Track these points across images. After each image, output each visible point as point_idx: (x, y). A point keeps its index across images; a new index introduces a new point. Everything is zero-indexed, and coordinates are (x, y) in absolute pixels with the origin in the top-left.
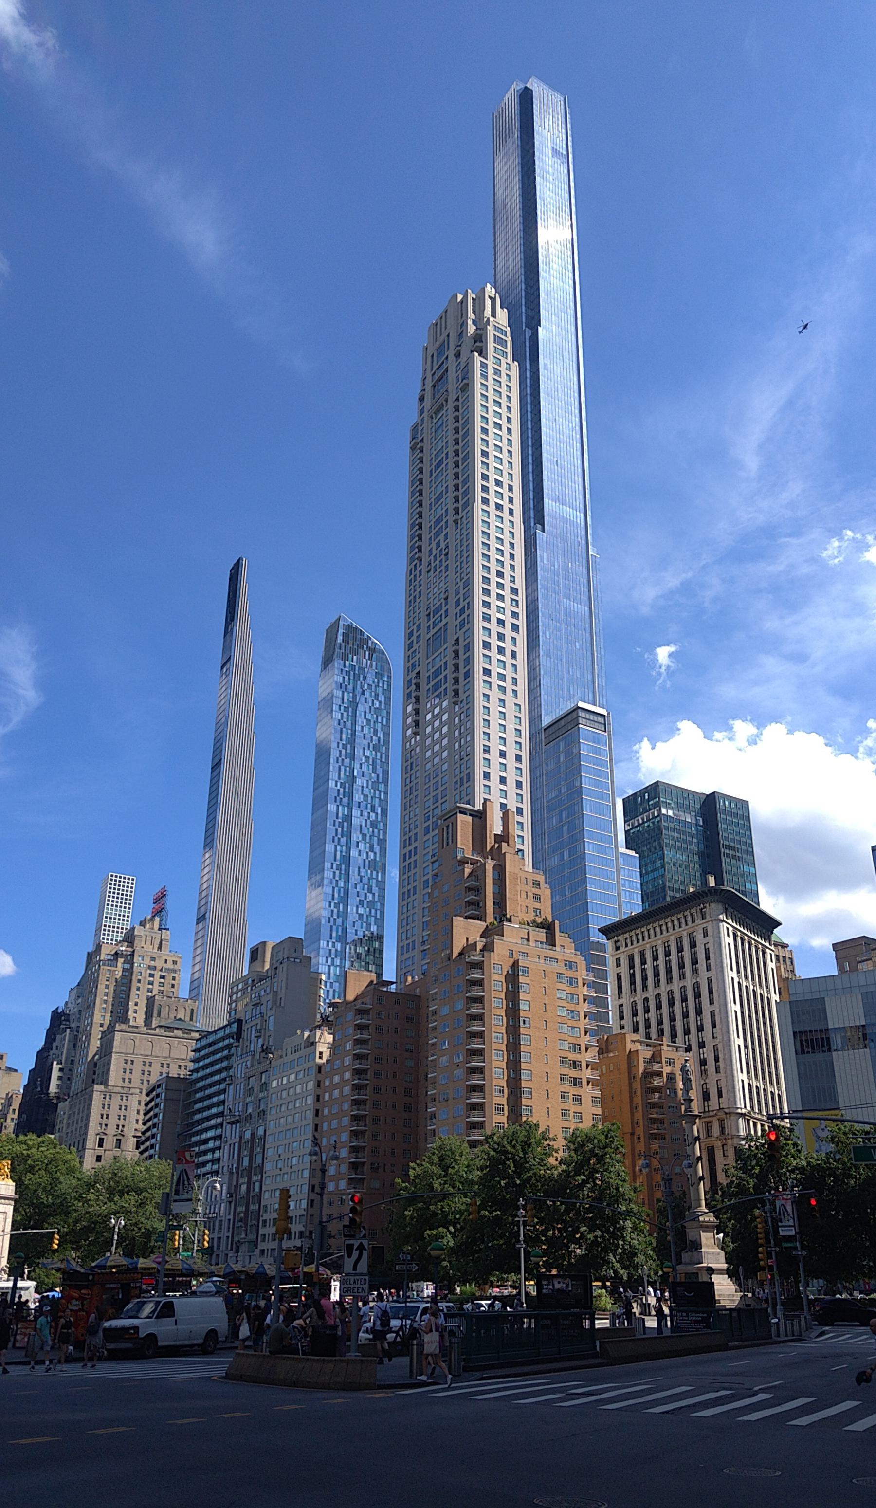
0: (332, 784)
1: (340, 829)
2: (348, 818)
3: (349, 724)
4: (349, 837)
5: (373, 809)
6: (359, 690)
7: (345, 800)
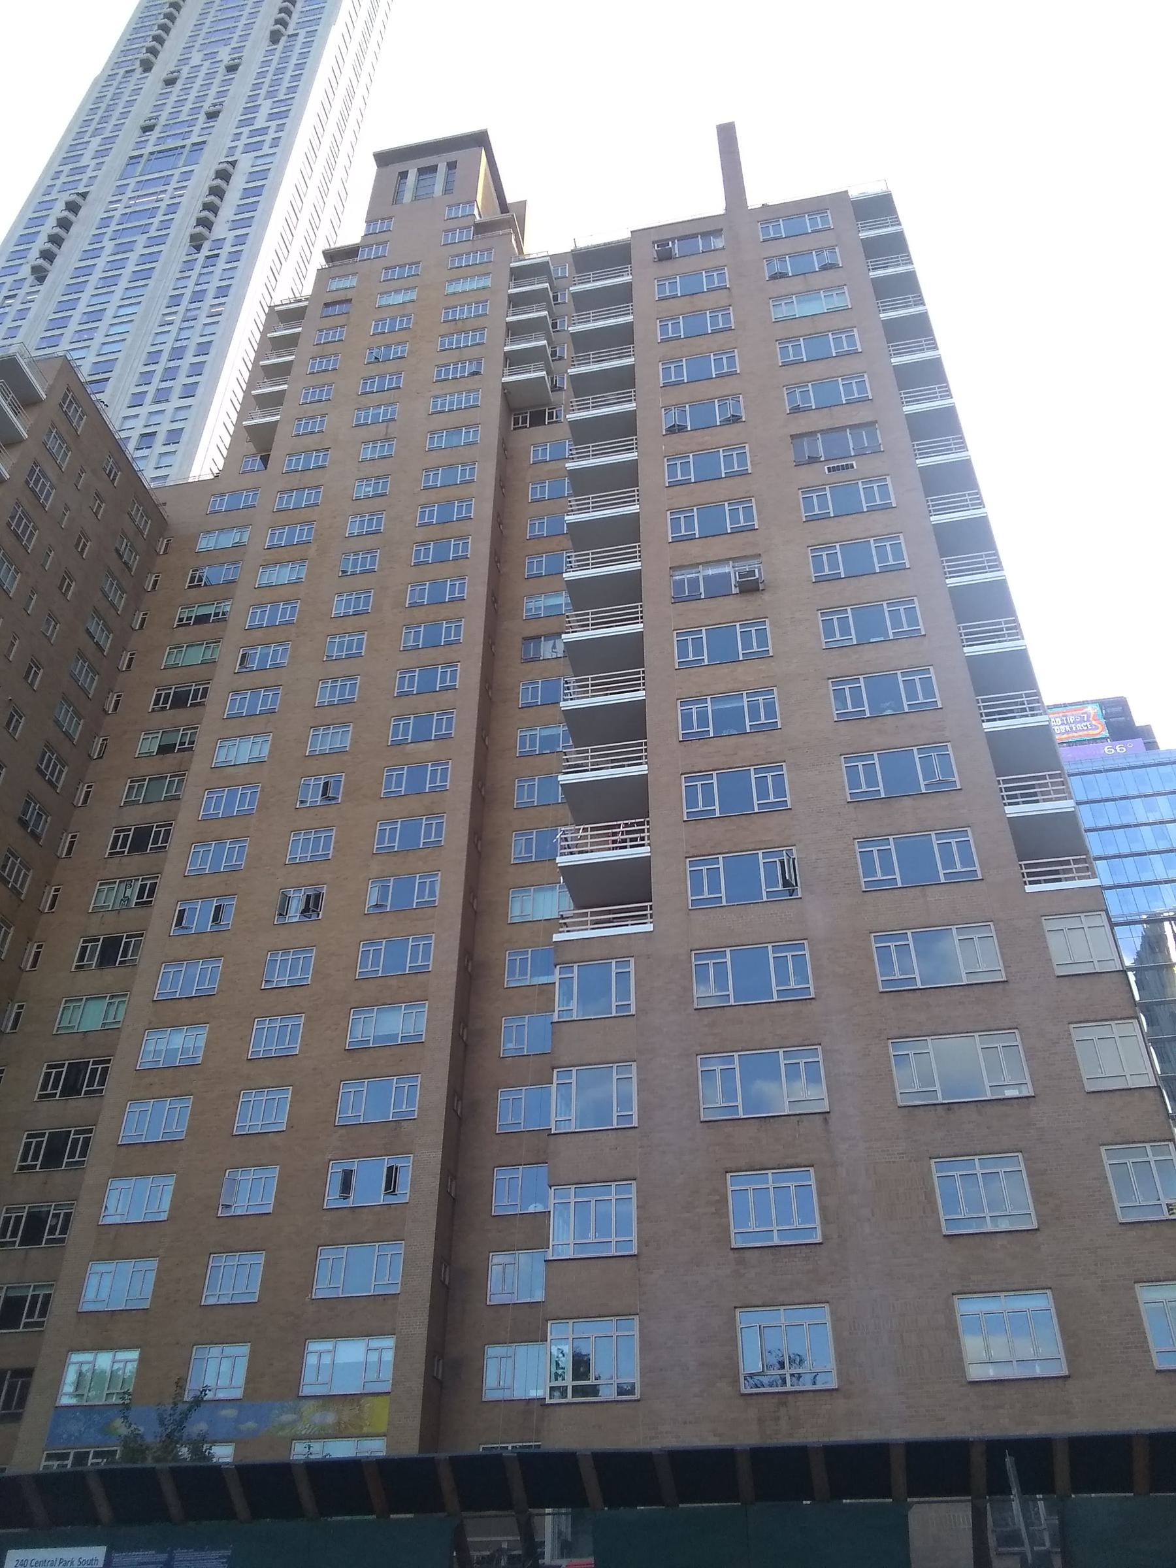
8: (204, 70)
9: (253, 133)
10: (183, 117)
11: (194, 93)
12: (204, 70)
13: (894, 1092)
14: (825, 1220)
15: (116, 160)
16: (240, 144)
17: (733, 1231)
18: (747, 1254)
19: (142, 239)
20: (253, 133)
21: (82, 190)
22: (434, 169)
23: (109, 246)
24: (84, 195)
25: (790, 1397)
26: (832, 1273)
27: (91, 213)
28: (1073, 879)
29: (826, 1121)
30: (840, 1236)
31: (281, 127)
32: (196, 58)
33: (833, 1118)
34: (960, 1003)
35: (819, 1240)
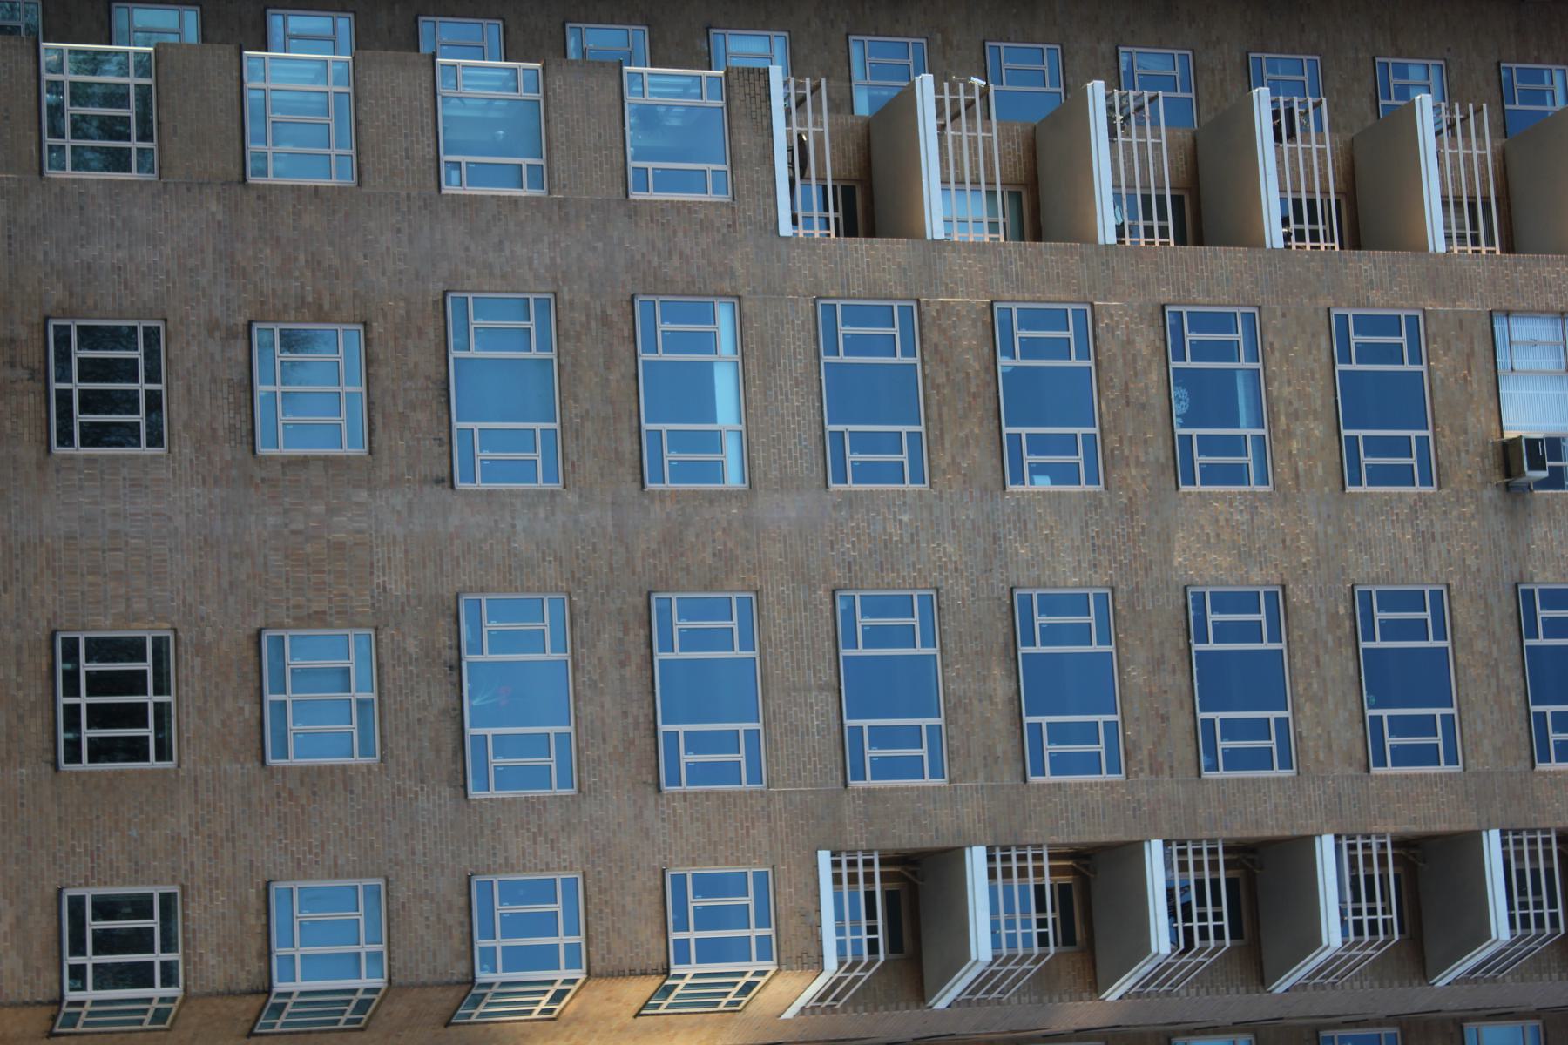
13: (482, 590)
14: (291, 463)
17: (277, 328)
18: (241, 344)
25: (40, 386)
26: (211, 462)
28: (840, 931)
29: (439, 481)
30: (263, 480)
33: (444, 493)
34: (625, 714)
35: (262, 451)
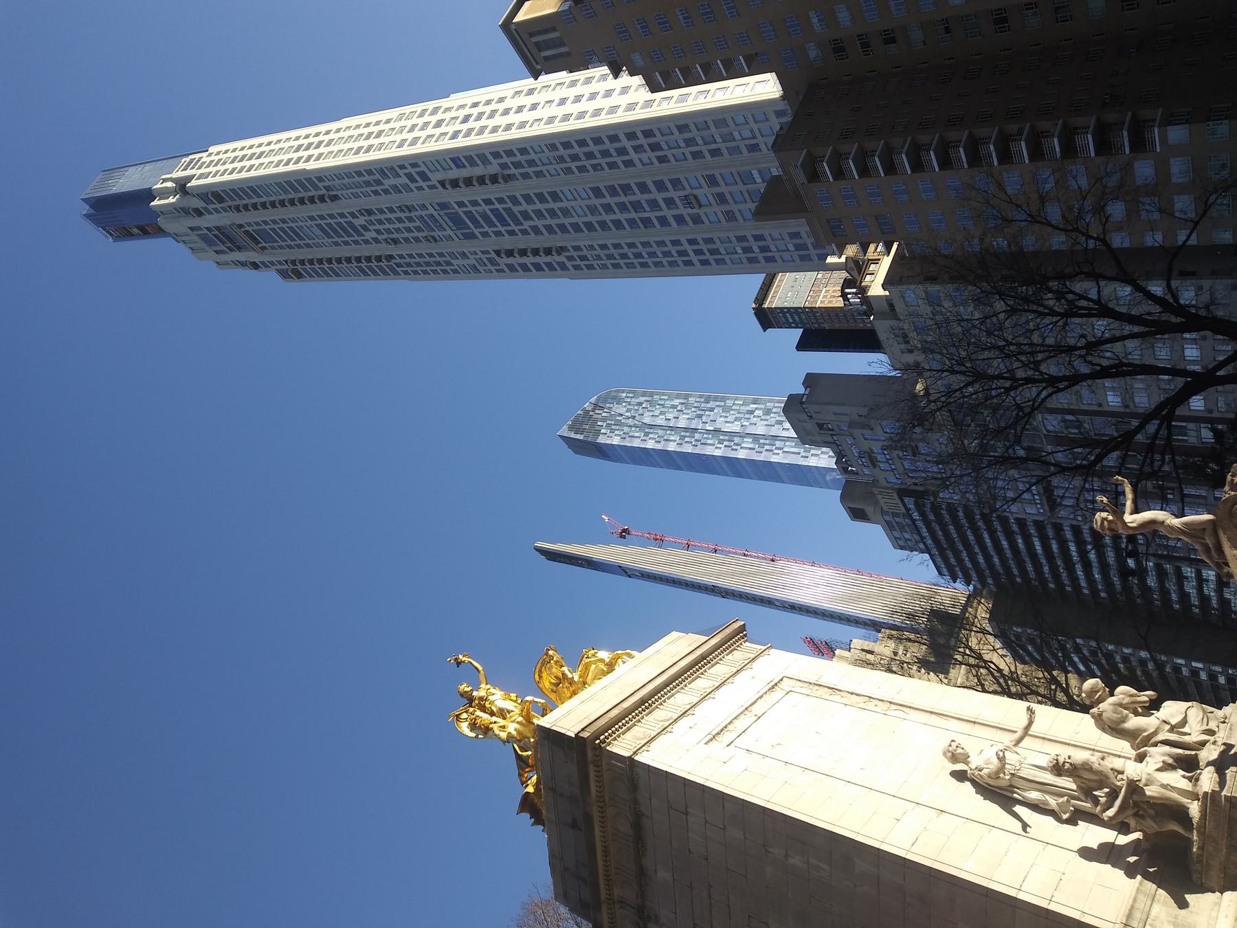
0: (718, 453)
1: (767, 447)
2: (756, 437)
3: (660, 432)
4: (775, 437)
5: (752, 412)
6: (630, 422)
7: (737, 440)
8: (378, 227)
9: (413, 180)
10: (418, 223)
11: (398, 225)
12: (378, 227)
15: (467, 246)
16: (424, 184)
19: (516, 209)
20: (413, 180)
21: (494, 255)
22: (536, 44)
23: (527, 225)
24: (498, 253)
27: (507, 242)
31: (402, 167)
32: (369, 235)
